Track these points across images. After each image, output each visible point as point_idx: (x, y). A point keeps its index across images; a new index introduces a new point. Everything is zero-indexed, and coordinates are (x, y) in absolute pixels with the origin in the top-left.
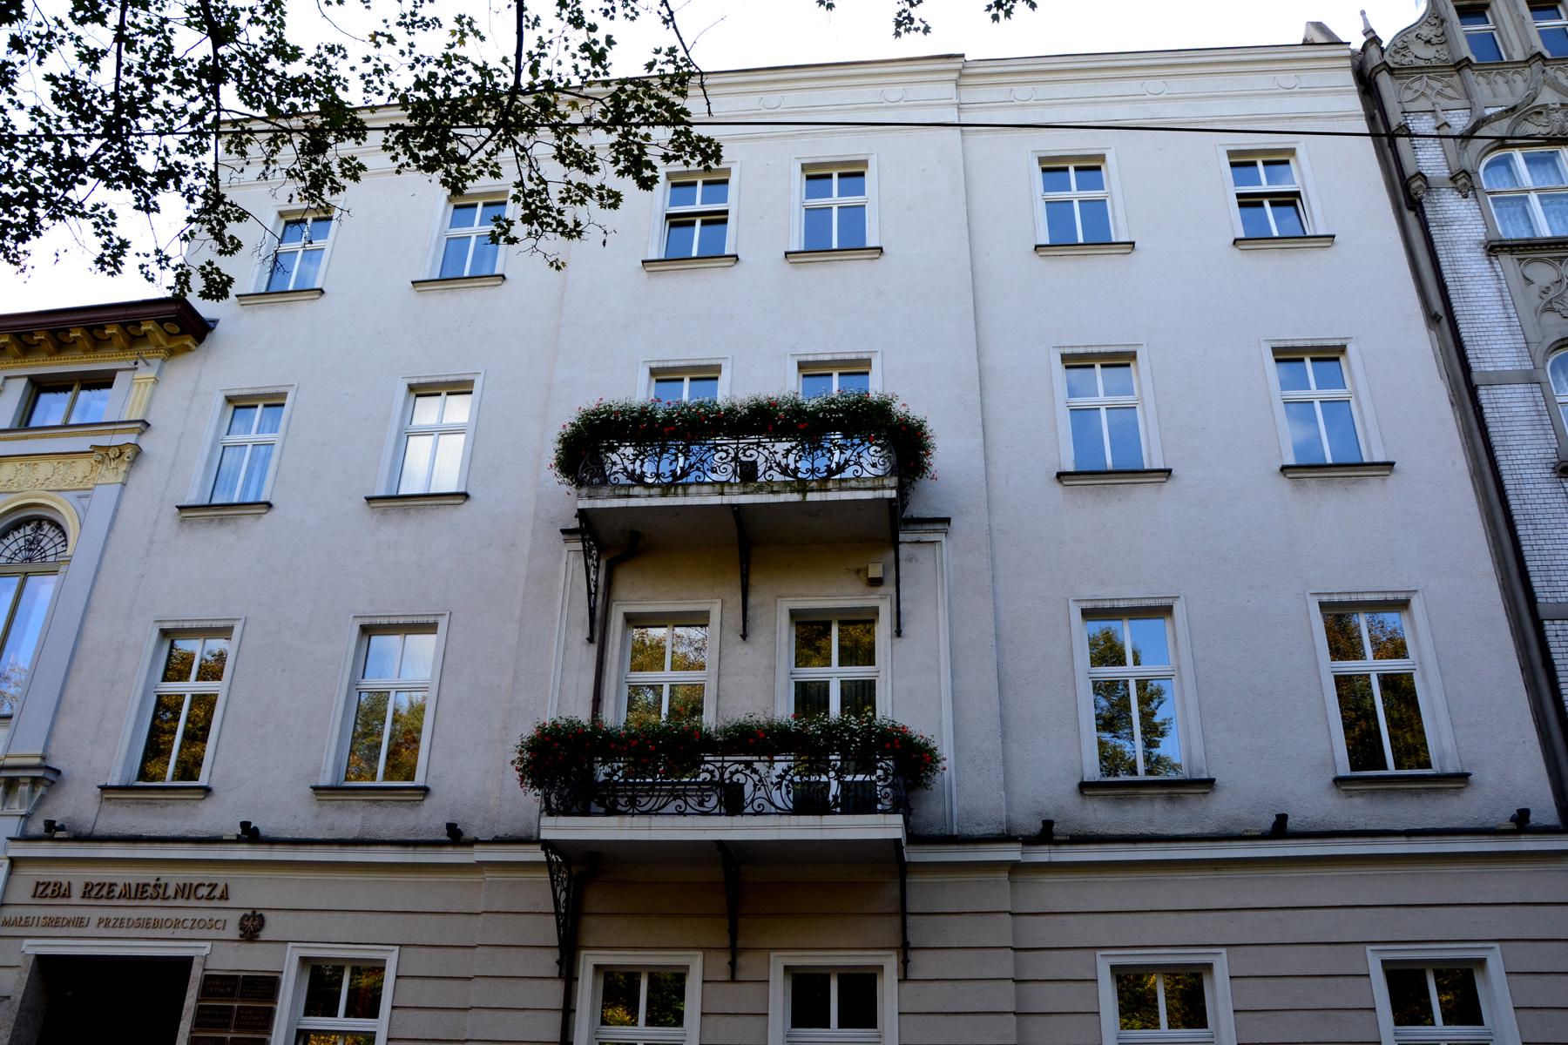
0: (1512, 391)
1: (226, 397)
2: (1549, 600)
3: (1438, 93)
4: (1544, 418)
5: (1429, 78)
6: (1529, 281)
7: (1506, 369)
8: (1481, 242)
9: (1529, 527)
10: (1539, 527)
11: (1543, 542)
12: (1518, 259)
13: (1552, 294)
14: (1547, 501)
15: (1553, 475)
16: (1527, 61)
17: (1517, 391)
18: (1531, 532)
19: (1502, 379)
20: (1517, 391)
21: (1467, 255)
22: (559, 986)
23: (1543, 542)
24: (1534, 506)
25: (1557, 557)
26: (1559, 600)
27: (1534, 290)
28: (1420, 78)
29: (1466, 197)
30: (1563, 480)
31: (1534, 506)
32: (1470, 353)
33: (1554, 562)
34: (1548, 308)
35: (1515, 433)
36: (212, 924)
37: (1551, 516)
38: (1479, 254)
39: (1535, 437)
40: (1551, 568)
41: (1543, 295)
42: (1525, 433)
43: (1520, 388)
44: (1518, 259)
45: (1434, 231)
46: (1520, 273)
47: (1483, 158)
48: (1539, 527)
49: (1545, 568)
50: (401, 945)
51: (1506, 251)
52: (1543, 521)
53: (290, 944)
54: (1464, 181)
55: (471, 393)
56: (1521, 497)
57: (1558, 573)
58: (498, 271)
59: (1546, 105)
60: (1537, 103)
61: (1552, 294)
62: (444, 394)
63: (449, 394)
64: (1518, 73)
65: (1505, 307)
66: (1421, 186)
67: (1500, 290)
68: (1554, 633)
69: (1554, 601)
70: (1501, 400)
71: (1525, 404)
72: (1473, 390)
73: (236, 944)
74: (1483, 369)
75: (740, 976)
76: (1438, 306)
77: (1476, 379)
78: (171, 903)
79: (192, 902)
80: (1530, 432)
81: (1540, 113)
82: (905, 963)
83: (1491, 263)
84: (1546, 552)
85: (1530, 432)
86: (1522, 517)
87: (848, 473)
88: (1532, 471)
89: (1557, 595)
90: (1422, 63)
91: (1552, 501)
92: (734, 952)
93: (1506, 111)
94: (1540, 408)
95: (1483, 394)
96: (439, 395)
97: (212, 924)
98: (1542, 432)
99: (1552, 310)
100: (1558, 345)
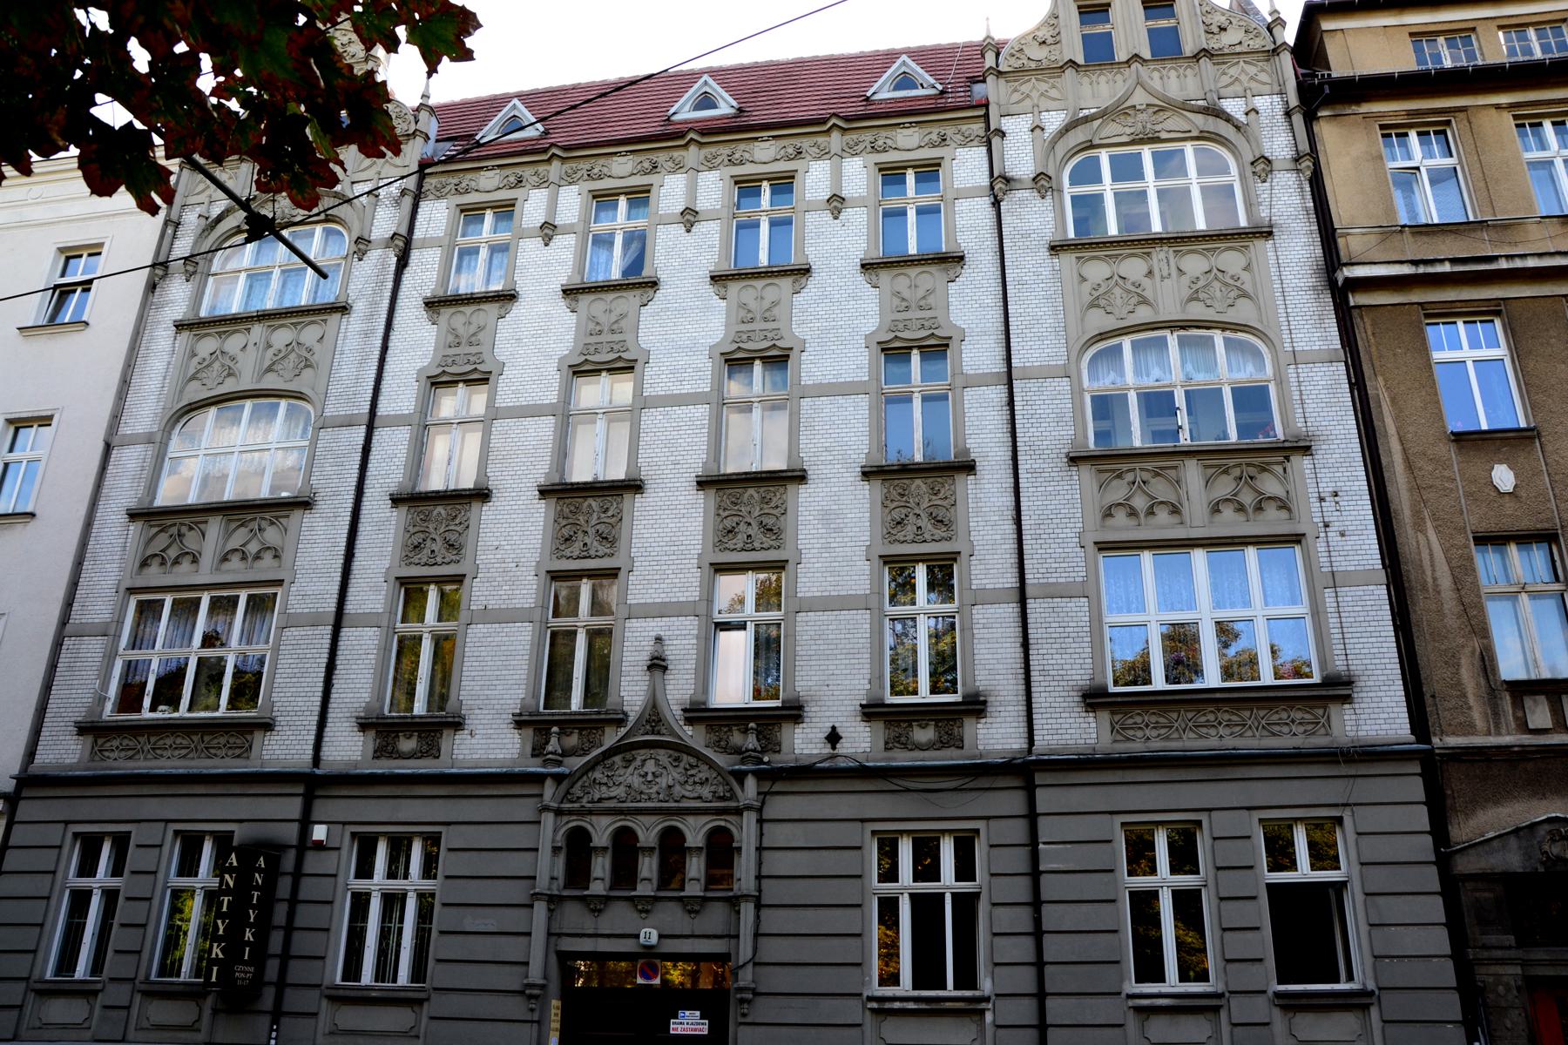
1: (7, 420)
3: (1042, 94)
5: (1037, 80)
6: (1083, 279)
12: (1175, 251)
13: (1201, 283)
16: (1127, 62)
27: (1087, 287)
28: (1030, 80)
34: (1093, 305)
41: (1094, 292)
44: (1175, 251)
46: (1075, 271)
47: (1066, 163)
54: (1263, 166)
55: (50, 425)
58: (84, 318)
59: (1135, 106)
61: (1201, 283)
62: (35, 426)
63: (40, 426)
64: (1121, 73)
66: (1308, 167)
69: (836, 593)
90: (1033, 65)
96: (32, 426)
99: (1197, 299)
100: (1099, 337)
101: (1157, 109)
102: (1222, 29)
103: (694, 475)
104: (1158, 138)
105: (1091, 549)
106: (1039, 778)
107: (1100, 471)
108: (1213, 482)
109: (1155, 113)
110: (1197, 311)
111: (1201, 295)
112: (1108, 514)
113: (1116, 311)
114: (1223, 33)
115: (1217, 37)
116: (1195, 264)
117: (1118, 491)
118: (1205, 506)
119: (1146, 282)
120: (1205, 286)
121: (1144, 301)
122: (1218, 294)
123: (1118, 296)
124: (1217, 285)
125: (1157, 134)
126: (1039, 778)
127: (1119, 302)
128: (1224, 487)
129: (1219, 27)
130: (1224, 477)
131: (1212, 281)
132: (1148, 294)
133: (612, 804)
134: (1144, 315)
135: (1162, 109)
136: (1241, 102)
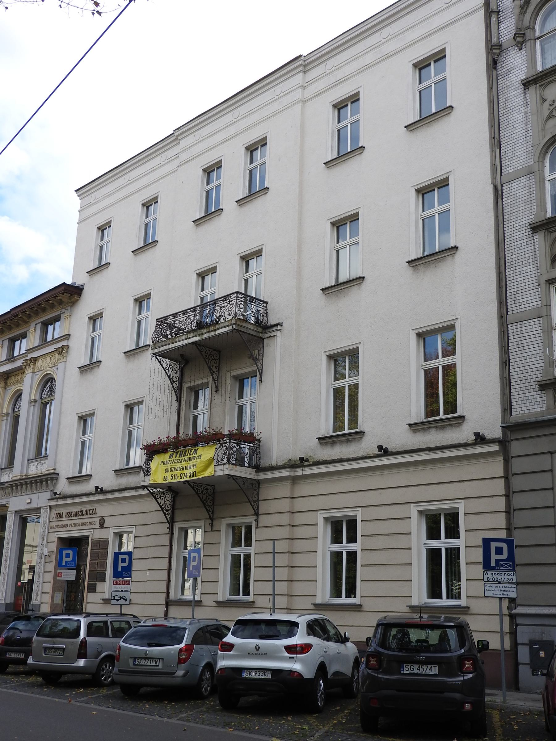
2: (514, 312)
17: (522, 181)
20: (522, 181)
22: (168, 536)
36: (90, 523)
39: (525, 210)
40: (518, 292)
48: (516, 268)
50: (136, 525)
53: (111, 528)
67: (526, 113)
68: (512, 331)
70: (513, 190)
73: (99, 529)
74: (507, 172)
75: (214, 529)
78: (84, 517)
79: (89, 516)
82: (257, 521)
87: (222, 320)
92: (212, 519)
97: (90, 523)
103: (528, 224)
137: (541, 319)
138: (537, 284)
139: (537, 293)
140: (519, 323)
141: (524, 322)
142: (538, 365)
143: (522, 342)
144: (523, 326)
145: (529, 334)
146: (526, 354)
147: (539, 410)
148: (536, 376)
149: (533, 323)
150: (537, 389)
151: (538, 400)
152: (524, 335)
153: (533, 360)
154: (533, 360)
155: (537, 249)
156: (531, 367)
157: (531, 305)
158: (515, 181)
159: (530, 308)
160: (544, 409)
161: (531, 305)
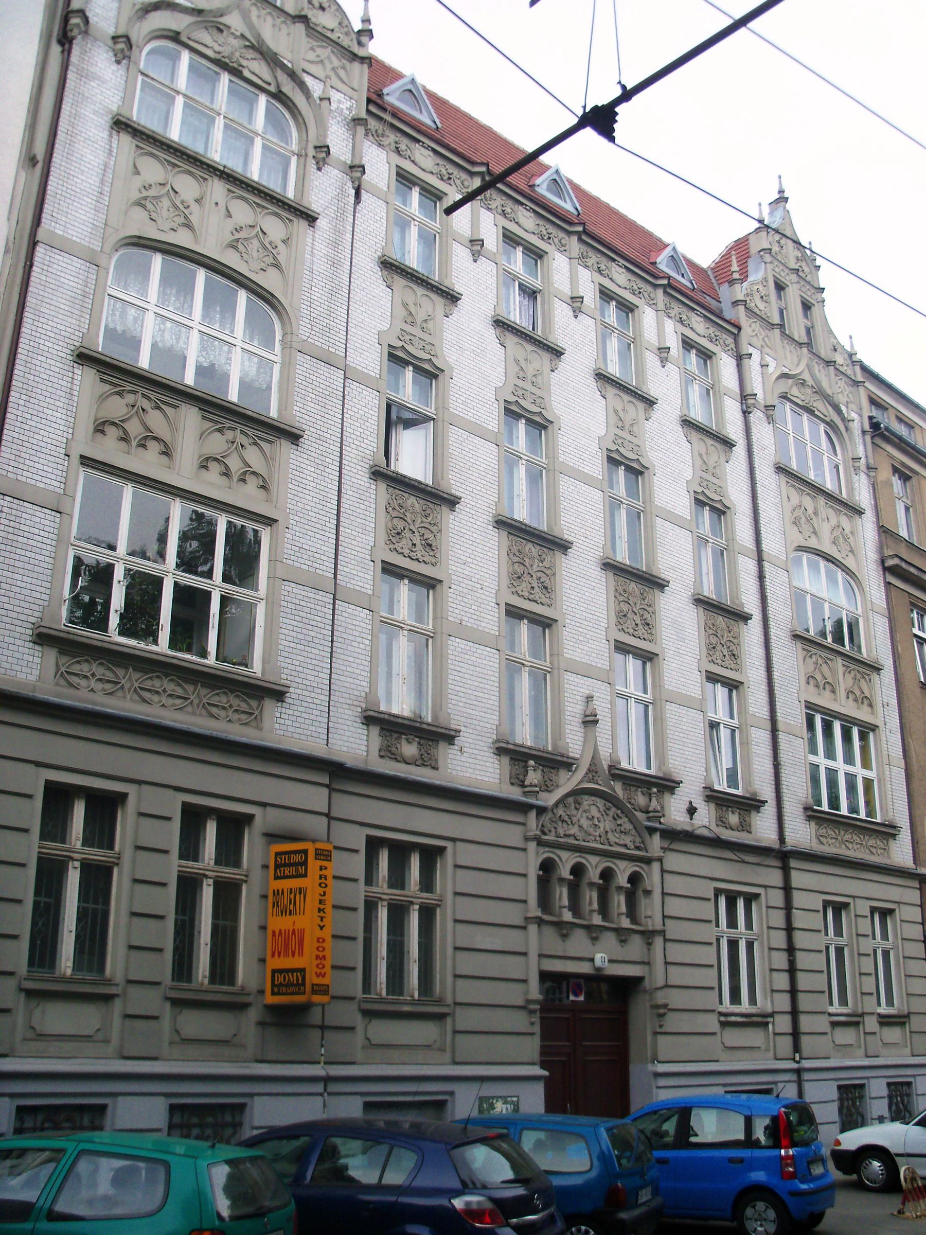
0: (69, 262)
2: (9, 475)
4: (87, 300)
7: (74, 239)
8: (111, 111)
9: (23, 397)
10: (32, 400)
11: (29, 416)
14: (51, 379)
15: (70, 358)
17: (74, 264)
18: (22, 402)
19: (64, 247)
20: (74, 264)
21: (91, 115)
23: (29, 416)
24: (37, 379)
25: (36, 436)
26: (19, 477)
29: (118, 62)
30: (76, 365)
31: (37, 379)
32: (47, 207)
33: (31, 440)
35: (53, 302)
37: (48, 394)
38: (105, 122)
39: (70, 314)
40: (25, 444)
41: (143, 190)
42: (62, 306)
43: (78, 263)
45: (71, 76)
47: (150, 40)
48: (32, 400)
49: (20, 442)
51: (129, 132)
52: (38, 397)
56: (29, 365)
57: (30, 451)
60: (221, 20)
65: (102, 182)
67: (106, 165)
70: (55, 266)
71: (76, 280)
72: (33, 244)
74: (52, 229)
76: (40, 150)
77: (41, 235)
80: (67, 308)
81: (221, 31)
83: (111, 136)
84: (27, 427)
85: (67, 308)
86: (21, 385)
88: (51, 345)
89: (19, 472)
91: (56, 380)
93: (193, 10)
94: (87, 290)
95: (40, 250)
98: (78, 313)
101: (247, 43)
102: (322, 8)
104: (241, 72)
105: (75, 459)
106: (793, 863)
107: (102, 380)
108: (206, 437)
109: (246, 47)
110: (231, 259)
111: (240, 247)
112: (100, 428)
113: (159, 220)
114: (320, 12)
115: (315, 11)
116: (243, 213)
117: (117, 407)
118: (196, 457)
119: (194, 207)
120: (246, 239)
121: (188, 225)
122: (255, 254)
123: (165, 208)
124: (256, 243)
125: (240, 68)
126: (793, 863)
127: (165, 213)
128: (217, 444)
129: (320, 4)
130: (217, 434)
131: (253, 238)
132: (194, 219)
133: (572, 841)
134: (182, 239)
135: (252, 47)
136: (321, 85)
137: (58, 515)
138: (63, 451)
139: (60, 467)
140: (15, 501)
141: (26, 504)
142: (38, 595)
143: (15, 538)
144: (23, 509)
145: (32, 530)
146: (17, 564)
147: (23, 676)
148: (30, 612)
149: (43, 516)
150: (28, 638)
151: (26, 657)
152: (22, 527)
153: (29, 580)
154: (29, 580)
155: (76, 393)
156: (24, 591)
157: (44, 480)
158: (63, 253)
159: (42, 486)
160: (33, 678)
161: (44, 480)
